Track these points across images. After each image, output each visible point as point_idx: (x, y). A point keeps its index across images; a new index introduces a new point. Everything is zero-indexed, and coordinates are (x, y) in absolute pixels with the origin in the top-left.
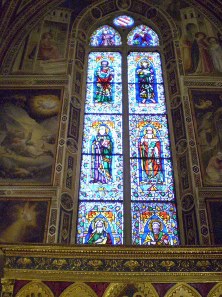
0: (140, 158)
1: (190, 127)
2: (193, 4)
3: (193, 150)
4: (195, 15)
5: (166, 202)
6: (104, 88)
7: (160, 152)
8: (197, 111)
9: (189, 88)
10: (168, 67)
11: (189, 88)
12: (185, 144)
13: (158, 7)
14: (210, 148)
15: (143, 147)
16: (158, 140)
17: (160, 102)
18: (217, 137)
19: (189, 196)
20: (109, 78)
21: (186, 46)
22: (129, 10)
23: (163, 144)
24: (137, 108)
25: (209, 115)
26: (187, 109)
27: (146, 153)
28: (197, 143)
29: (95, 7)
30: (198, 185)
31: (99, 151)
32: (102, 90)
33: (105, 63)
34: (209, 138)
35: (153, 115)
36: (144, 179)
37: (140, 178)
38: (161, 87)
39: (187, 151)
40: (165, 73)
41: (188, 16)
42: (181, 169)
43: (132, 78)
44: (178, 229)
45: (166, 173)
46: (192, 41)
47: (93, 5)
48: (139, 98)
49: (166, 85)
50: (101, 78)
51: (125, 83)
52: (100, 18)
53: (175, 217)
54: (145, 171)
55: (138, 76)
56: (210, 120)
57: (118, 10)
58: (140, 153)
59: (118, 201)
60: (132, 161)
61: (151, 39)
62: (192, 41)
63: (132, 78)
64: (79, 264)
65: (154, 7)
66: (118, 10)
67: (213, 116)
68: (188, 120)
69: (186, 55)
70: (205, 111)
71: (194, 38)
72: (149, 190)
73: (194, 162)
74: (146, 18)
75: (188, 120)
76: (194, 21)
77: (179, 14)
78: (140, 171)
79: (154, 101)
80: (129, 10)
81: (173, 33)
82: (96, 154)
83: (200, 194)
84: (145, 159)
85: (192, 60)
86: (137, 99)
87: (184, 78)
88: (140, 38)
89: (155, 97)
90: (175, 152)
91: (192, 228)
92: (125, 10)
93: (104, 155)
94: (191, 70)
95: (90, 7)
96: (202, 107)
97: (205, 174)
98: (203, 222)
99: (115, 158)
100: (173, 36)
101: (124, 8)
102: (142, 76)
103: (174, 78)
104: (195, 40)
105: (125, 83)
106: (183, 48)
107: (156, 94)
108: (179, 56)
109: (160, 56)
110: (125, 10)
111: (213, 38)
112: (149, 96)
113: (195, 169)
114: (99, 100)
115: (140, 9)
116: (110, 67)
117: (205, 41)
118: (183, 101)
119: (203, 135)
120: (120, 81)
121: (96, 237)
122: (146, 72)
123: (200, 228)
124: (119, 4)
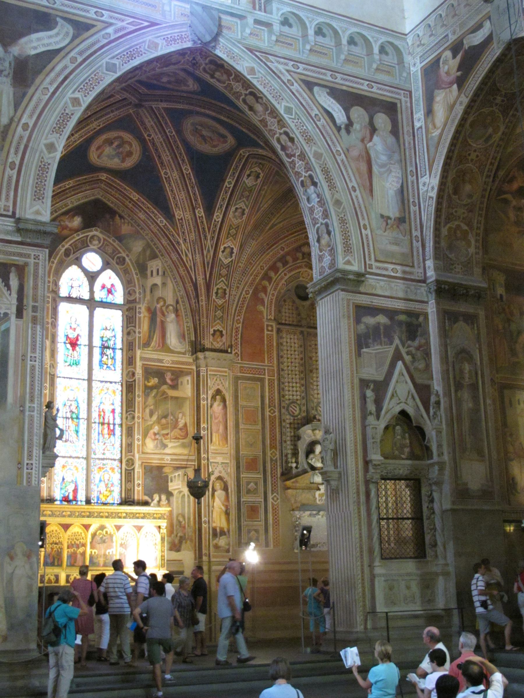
0: (99, 423)
1: (139, 403)
2: (162, 255)
3: (139, 423)
4: (160, 273)
5: (115, 460)
6: (73, 350)
7: (114, 419)
8: (146, 387)
9: (143, 364)
10: (129, 334)
11: (143, 364)
12: (133, 418)
13: (128, 256)
14: (151, 423)
15: (102, 414)
16: (113, 407)
17: (117, 368)
18: (157, 413)
19: (131, 459)
20: (77, 339)
21: (146, 314)
22: (99, 248)
23: (116, 411)
24: (98, 373)
25: (154, 392)
26: (139, 386)
27: (104, 418)
28: (143, 418)
29: (67, 246)
30: (138, 452)
31: (69, 415)
32: (71, 351)
33: (73, 320)
34: (151, 415)
35: (111, 382)
36: (101, 441)
37: (99, 440)
38: (120, 351)
39: (134, 424)
40: (125, 339)
41: (155, 273)
42: (128, 436)
43: (97, 342)
44: (121, 480)
45: (116, 436)
46: (153, 309)
47: (67, 243)
48: (101, 364)
49: (125, 353)
50: (70, 339)
51: (91, 347)
52: (71, 256)
53: (120, 471)
54: (102, 434)
55: (102, 337)
56: (155, 397)
57: (88, 246)
58: (99, 418)
59: (83, 458)
60: (93, 425)
61: (115, 291)
62: (153, 309)
63: (97, 342)
64: (77, 514)
65: (124, 255)
66: (88, 246)
67: (157, 394)
68: (139, 396)
69: (145, 326)
70: (152, 388)
71: (155, 304)
72: (104, 450)
73: (139, 434)
74: (115, 263)
75: (139, 396)
76: (158, 280)
77: (147, 270)
78: (99, 434)
79: (113, 369)
80: (99, 248)
81: (137, 295)
82: (67, 418)
83: (140, 458)
84: (103, 424)
85: (150, 332)
86: (100, 365)
87: (141, 353)
88: (106, 290)
89: (114, 365)
90: (124, 420)
91: (131, 481)
92: (95, 247)
93: (72, 418)
94: (147, 344)
95: (63, 246)
96: (150, 384)
97: (144, 444)
98: (138, 479)
99: (81, 421)
100: (137, 300)
101: (94, 245)
102: (105, 339)
103: (132, 350)
104: (156, 307)
105: (91, 347)
106: (144, 317)
107: (115, 360)
108: (140, 327)
109: (123, 315)
110: (95, 247)
111: (171, 305)
112: (110, 362)
113: (138, 440)
114: (68, 364)
115: (110, 251)
116: (78, 325)
117: (164, 308)
118: (137, 376)
119: (147, 411)
120: (87, 343)
121: (67, 484)
122: (108, 334)
123: (136, 483)
124: (90, 241)
